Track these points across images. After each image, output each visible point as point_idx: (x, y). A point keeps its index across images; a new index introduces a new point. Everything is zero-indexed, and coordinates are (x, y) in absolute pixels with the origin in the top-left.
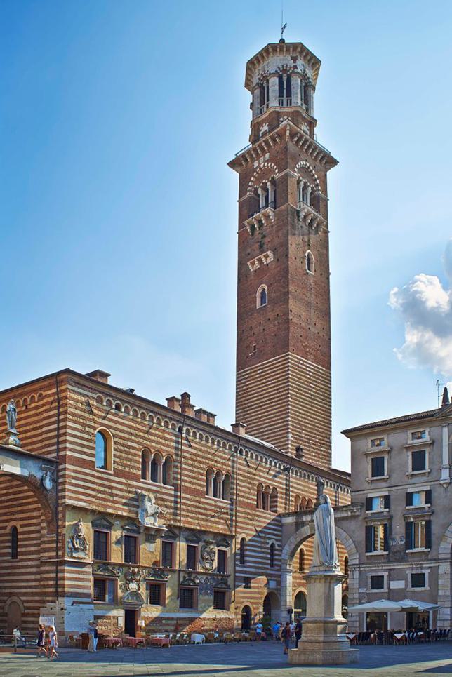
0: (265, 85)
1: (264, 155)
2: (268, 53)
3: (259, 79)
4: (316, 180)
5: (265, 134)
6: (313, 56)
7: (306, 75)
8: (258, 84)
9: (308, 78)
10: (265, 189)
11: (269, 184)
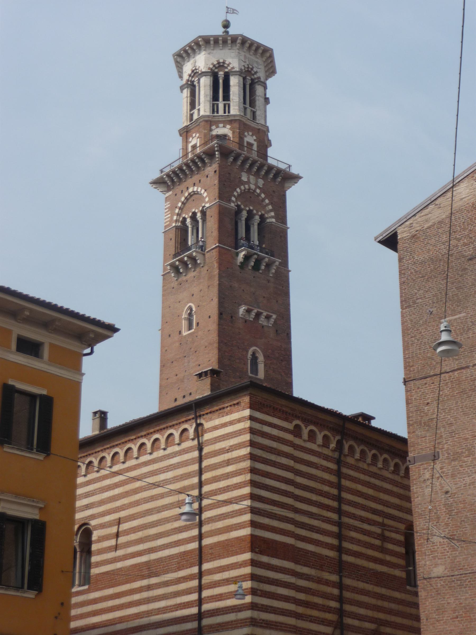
0: (197, 85)
3: (190, 76)
5: (194, 147)
6: (259, 46)
9: (256, 73)
11: (199, 215)
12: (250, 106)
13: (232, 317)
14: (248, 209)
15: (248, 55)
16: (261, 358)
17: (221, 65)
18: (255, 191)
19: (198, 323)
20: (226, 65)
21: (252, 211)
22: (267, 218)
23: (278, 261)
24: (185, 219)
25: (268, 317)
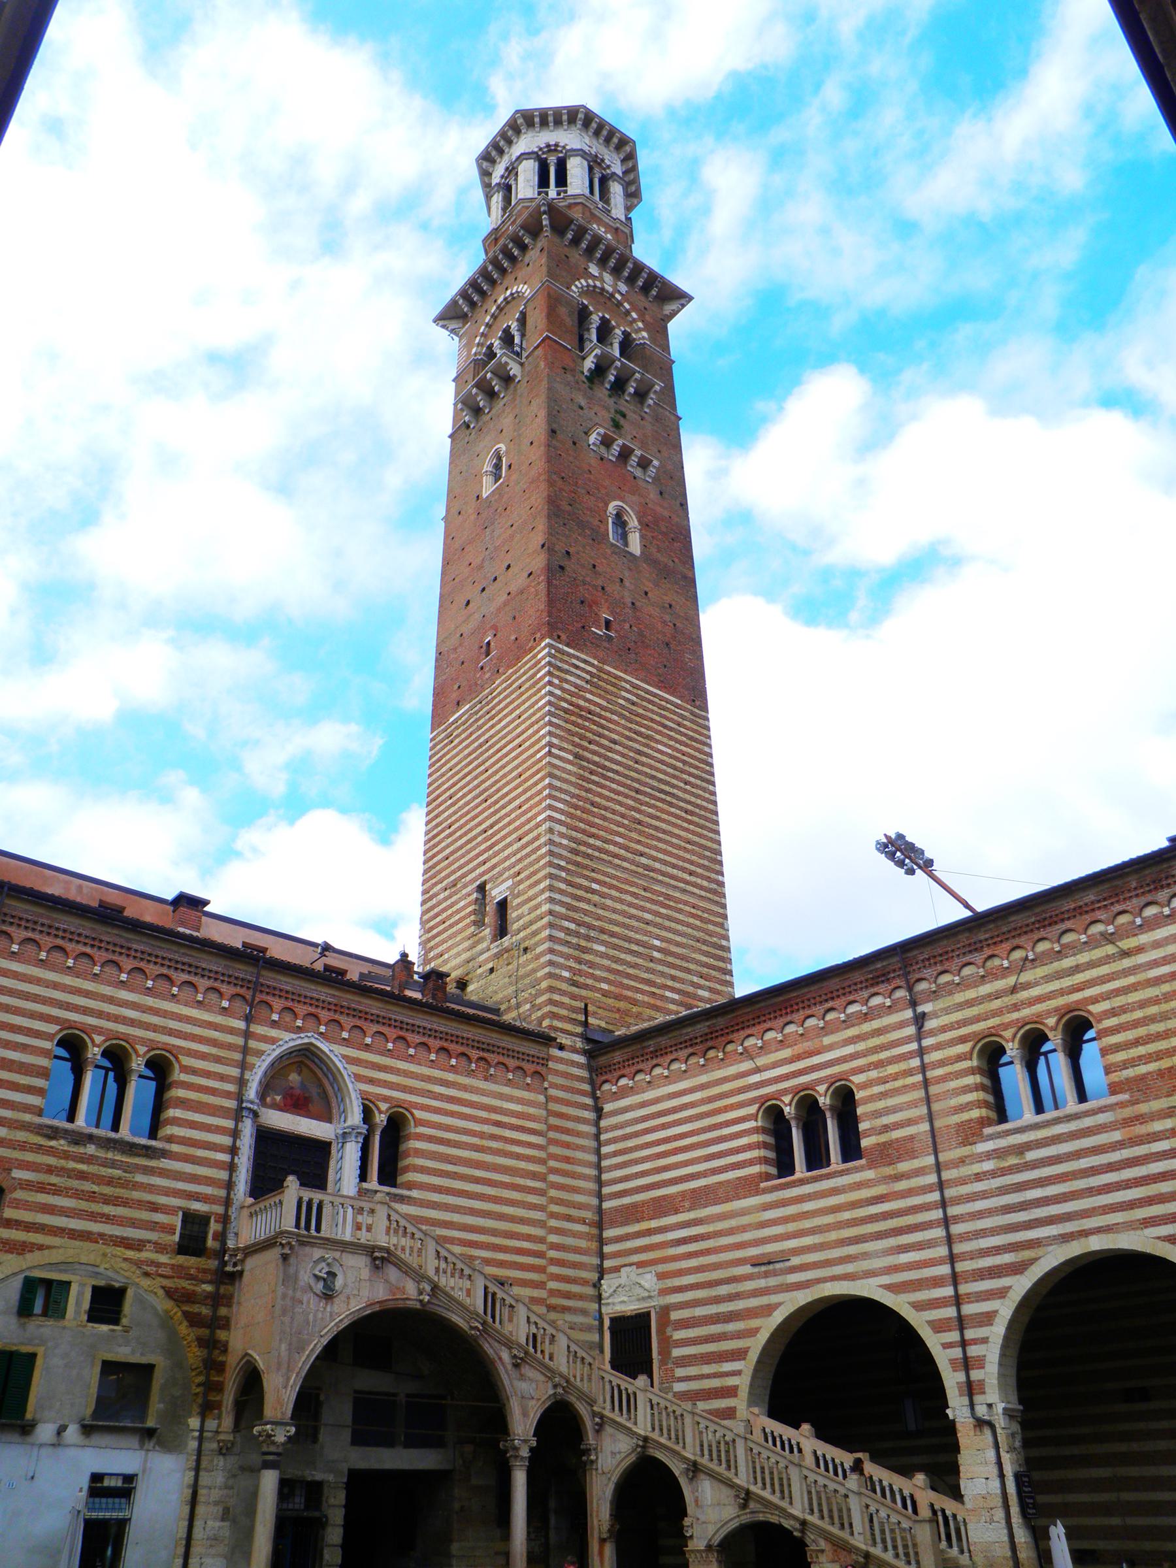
0: (512, 182)
2: (518, 132)
3: (502, 177)
4: (634, 321)
7: (603, 160)
8: (498, 184)
9: (609, 167)
10: (508, 339)
11: (514, 326)
13: (574, 443)
15: (595, 142)
16: (633, 522)
17: (552, 148)
18: (612, 295)
19: (510, 466)
21: (608, 321)
24: (490, 347)
25: (644, 464)
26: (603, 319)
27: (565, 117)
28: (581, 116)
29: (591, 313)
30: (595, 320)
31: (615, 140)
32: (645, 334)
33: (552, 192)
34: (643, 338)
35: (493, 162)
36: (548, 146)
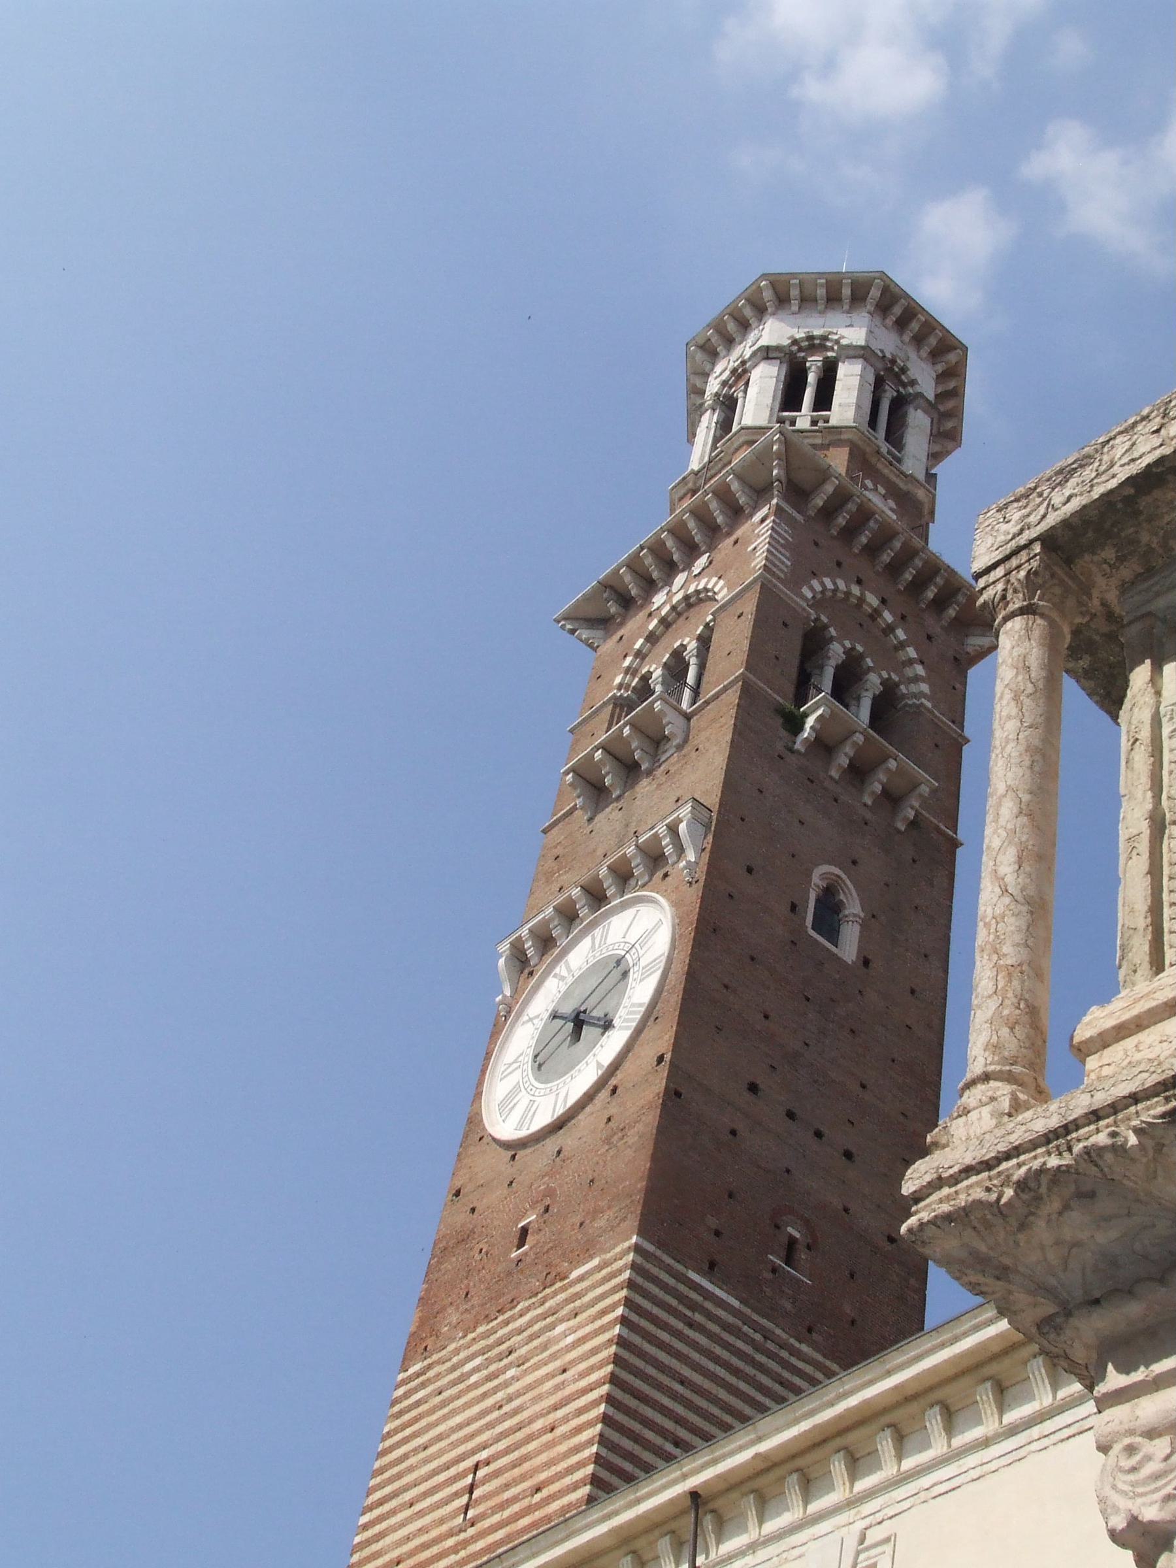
1: (688, 566)
2: (761, 311)
3: (724, 383)
6: (931, 326)
7: (904, 370)
9: (913, 383)
10: (676, 668)
11: (692, 645)
12: (887, 439)
14: (848, 644)
17: (814, 344)
20: (829, 344)
21: (861, 657)
22: (904, 696)
23: (927, 784)
24: (646, 678)
26: (849, 652)
27: (846, 292)
28: (875, 293)
29: (832, 639)
30: (836, 652)
31: (933, 341)
32: (925, 687)
33: (803, 419)
34: (922, 694)
35: (714, 356)
36: (810, 338)
